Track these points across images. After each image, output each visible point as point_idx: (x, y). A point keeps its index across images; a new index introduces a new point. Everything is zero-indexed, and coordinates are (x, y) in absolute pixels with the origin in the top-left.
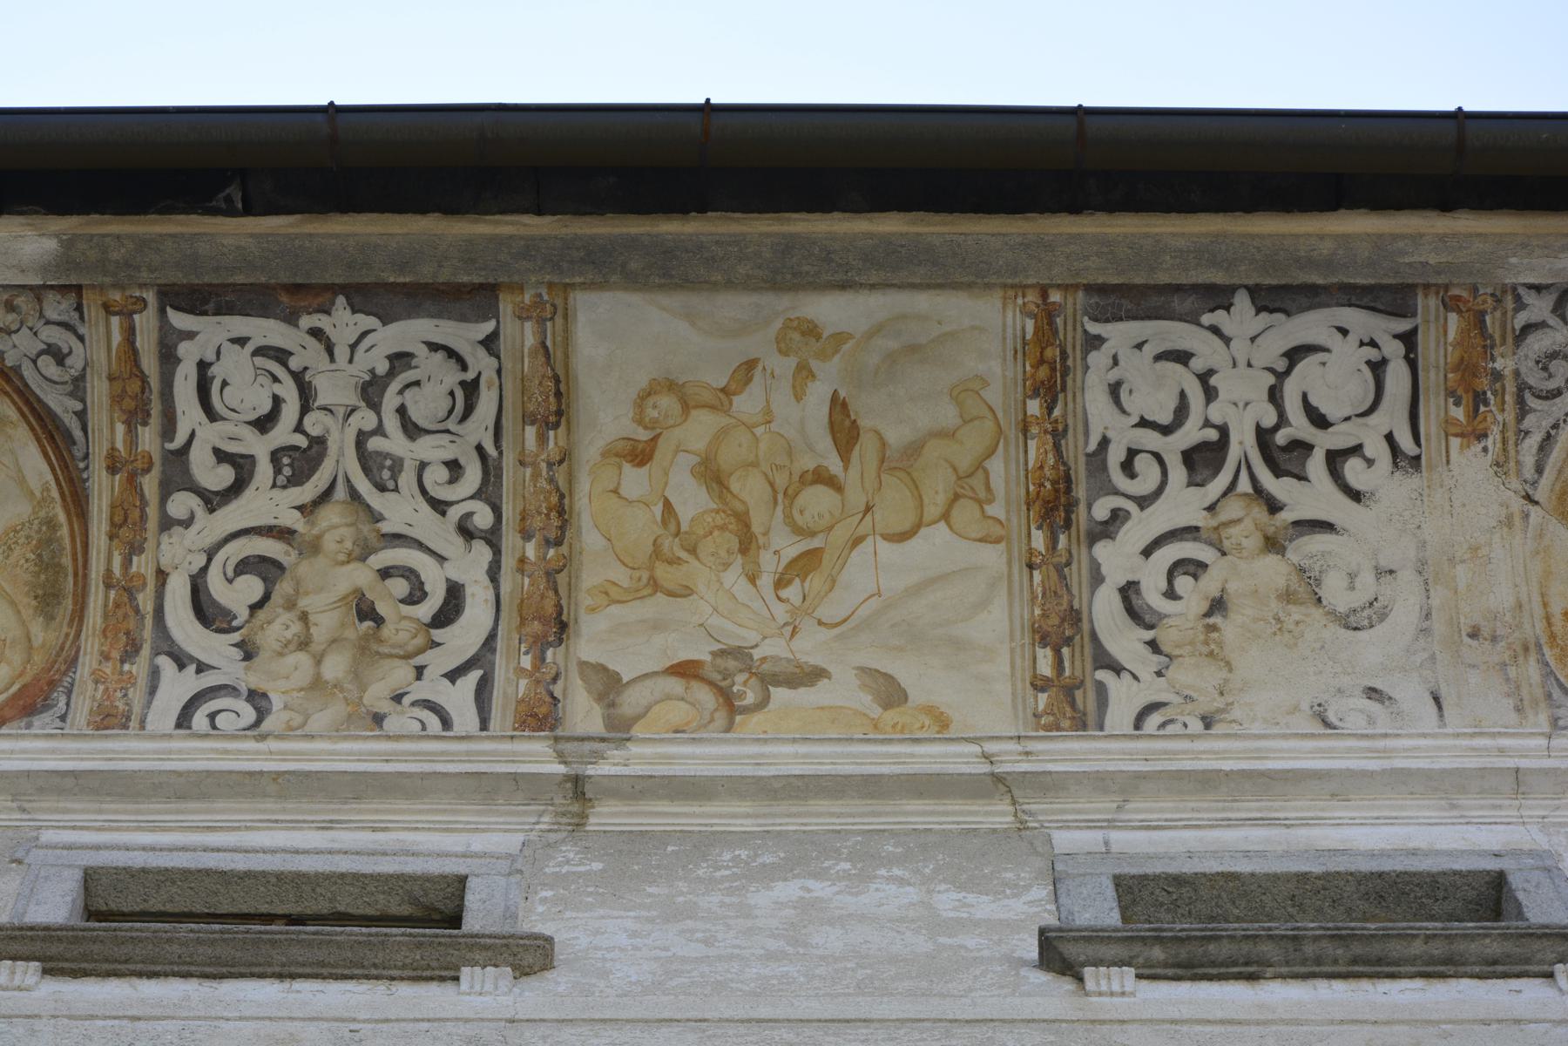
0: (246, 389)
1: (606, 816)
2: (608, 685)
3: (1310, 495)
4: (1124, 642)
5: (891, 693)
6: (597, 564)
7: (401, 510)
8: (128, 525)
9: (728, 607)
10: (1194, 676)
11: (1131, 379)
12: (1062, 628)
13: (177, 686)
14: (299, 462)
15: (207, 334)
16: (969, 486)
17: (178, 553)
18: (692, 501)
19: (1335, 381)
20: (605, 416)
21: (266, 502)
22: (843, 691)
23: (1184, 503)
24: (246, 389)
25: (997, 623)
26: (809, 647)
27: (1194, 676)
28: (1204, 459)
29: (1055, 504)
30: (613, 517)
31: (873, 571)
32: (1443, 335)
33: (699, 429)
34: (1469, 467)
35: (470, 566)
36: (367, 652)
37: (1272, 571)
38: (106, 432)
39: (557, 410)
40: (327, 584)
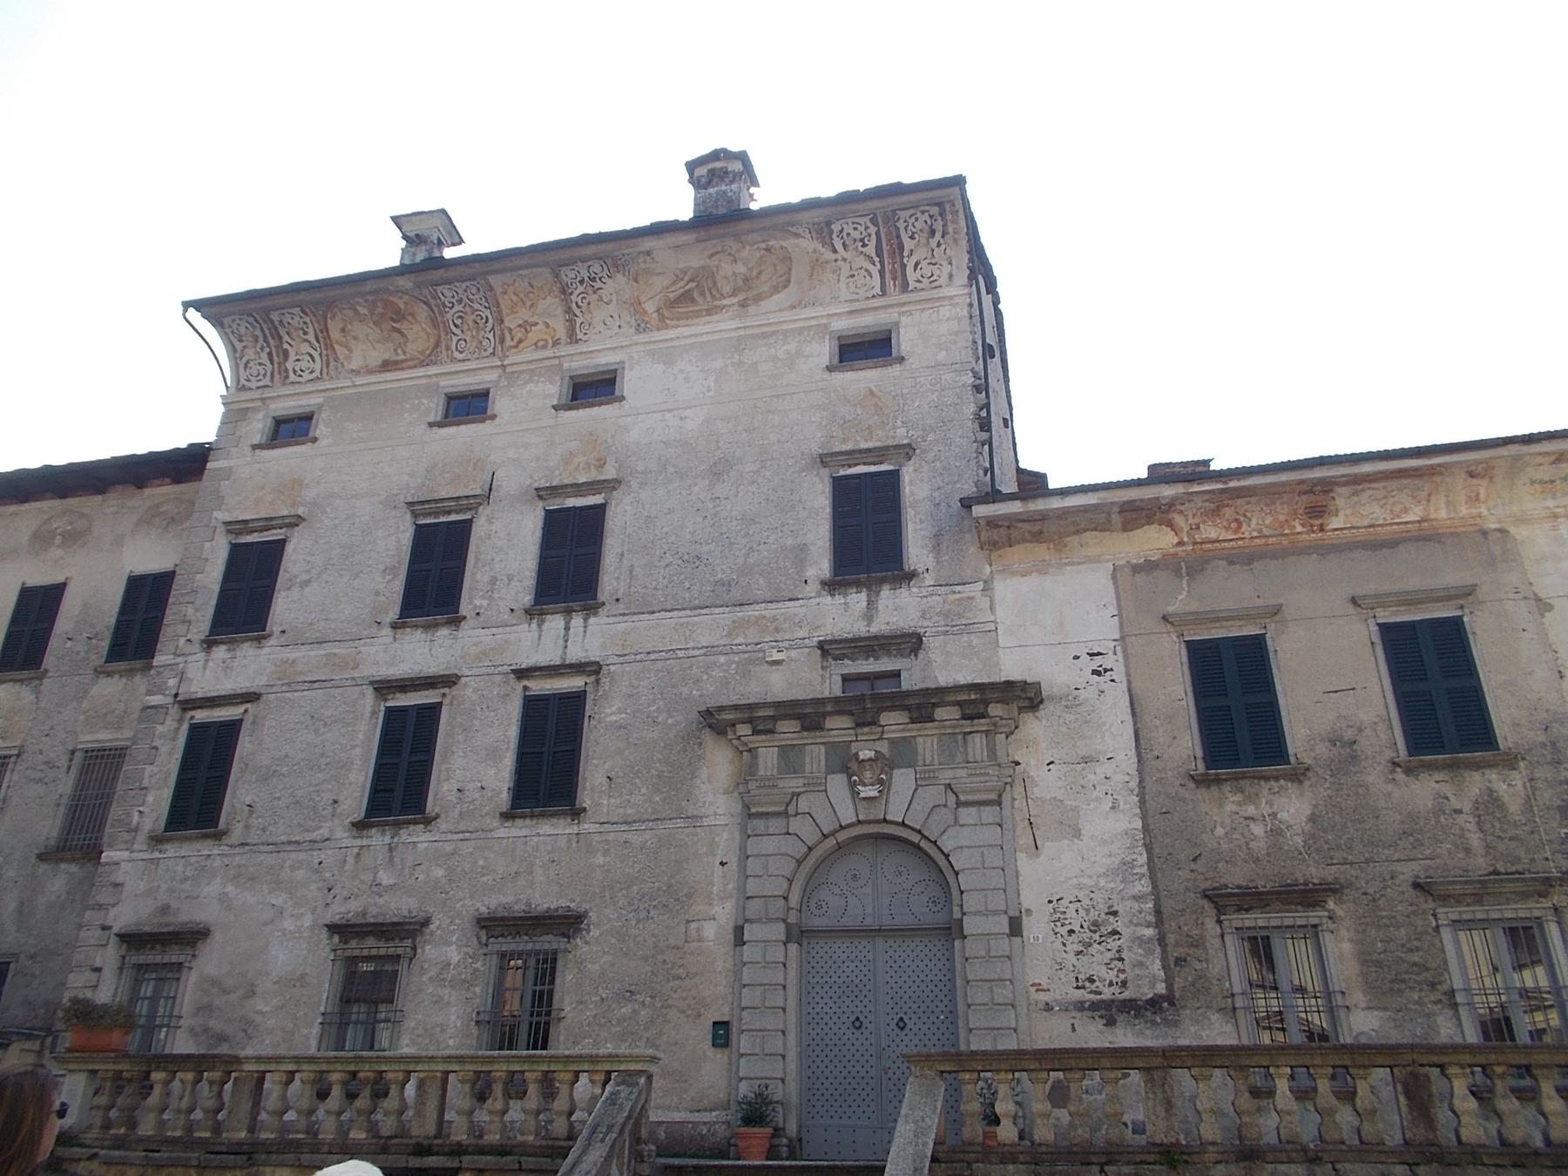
0: (448, 294)
1: (509, 369)
2: (510, 330)
3: (598, 284)
4: (577, 312)
5: (547, 325)
6: (505, 311)
7: (476, 306)
8: (442, 314)
9: (524, 314)
10: (587, 316)
11: (568, 275)
12: (569, 310)
13: (455, 339)
14: (460, 302)
15: (439, 289)
16: (551, 291)
17: (449, 316)
18: (514, 298)
19: (596, 268)
20: (499, 290)
21: (457, 308)
22: (541, 326)
23: (581, 289)
24: (448, 294)
25: (560, 311)
26: (535, 319)
27: (587, 316)
28: (582, 282)
29: (563, 291)
30: (505, 303)
31: (542, 305)
32: (609, 261)
33: (511, 289)
34: (619, 276)
35: (488, 313)
36: (478, 329)
37: (595, 297)
38: (433, 302)
39: (491, 289)
40: (470, 318)
